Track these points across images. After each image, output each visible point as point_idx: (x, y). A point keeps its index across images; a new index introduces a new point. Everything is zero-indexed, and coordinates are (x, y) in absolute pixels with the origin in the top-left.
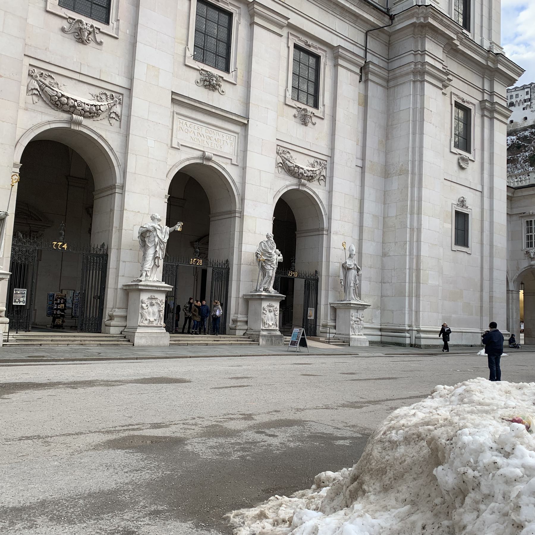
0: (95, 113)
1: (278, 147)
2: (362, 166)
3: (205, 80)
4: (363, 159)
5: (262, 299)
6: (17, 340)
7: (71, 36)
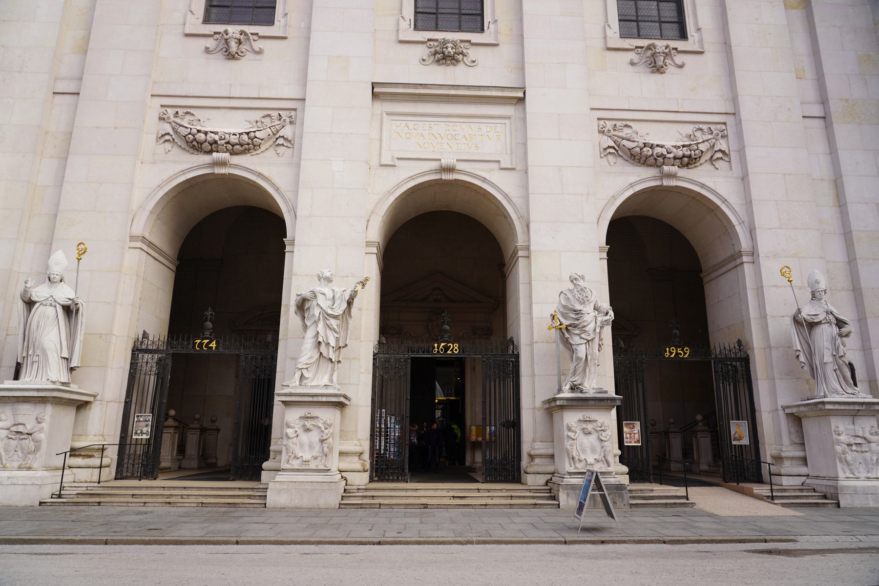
0: (248, 144)
1: (602, 122)
2: (823, 116)
3: (436, 53)
4: (824, 101)
5: (562, 407)
6: (78, 494)
7: (220, 55)
